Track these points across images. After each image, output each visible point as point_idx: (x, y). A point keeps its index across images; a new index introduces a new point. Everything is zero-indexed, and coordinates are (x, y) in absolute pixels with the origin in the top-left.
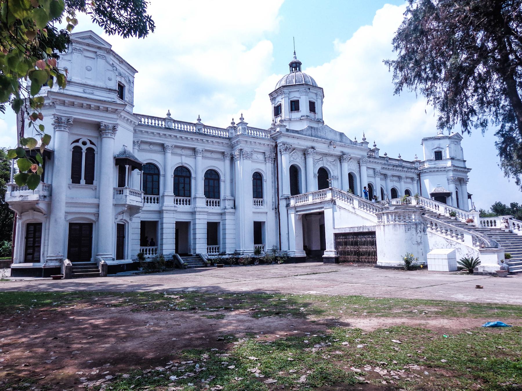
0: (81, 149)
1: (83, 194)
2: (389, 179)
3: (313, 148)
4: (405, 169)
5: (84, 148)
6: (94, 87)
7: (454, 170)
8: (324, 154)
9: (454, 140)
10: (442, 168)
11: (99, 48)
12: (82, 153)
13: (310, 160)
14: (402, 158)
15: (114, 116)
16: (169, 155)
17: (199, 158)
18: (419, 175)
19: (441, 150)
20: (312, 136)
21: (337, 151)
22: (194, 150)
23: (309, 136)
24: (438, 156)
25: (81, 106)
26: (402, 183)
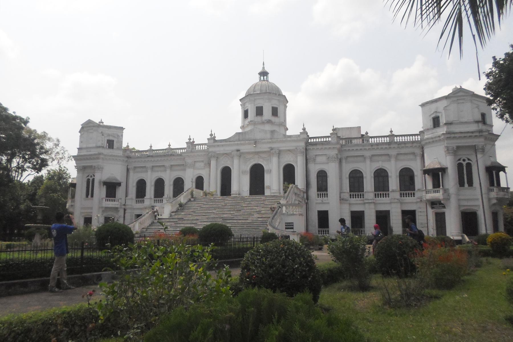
0: (89, 180)
1: (88, 203)
2: (367, 160)
3: (238, 151)
4: (392, 146)
5: (91, 179)
6: (91, 148)
7: (448, 138)
8: (255, 152)
9: (455, 99)
10: (435, 137)
11: (94, 126)
12: (89, 182)
13: (236, 161)
14: (393, 133)
15: (98, 161)
16: (149, 172)
17: (168, 171)
18: (423, 148)
19: (438, 114)
20: (239, 140)
21: (264, 147)
22: (164, 166)
23: (236, 141)
24: (436, 122)
25: (84, 159)
26: (393, 161)
